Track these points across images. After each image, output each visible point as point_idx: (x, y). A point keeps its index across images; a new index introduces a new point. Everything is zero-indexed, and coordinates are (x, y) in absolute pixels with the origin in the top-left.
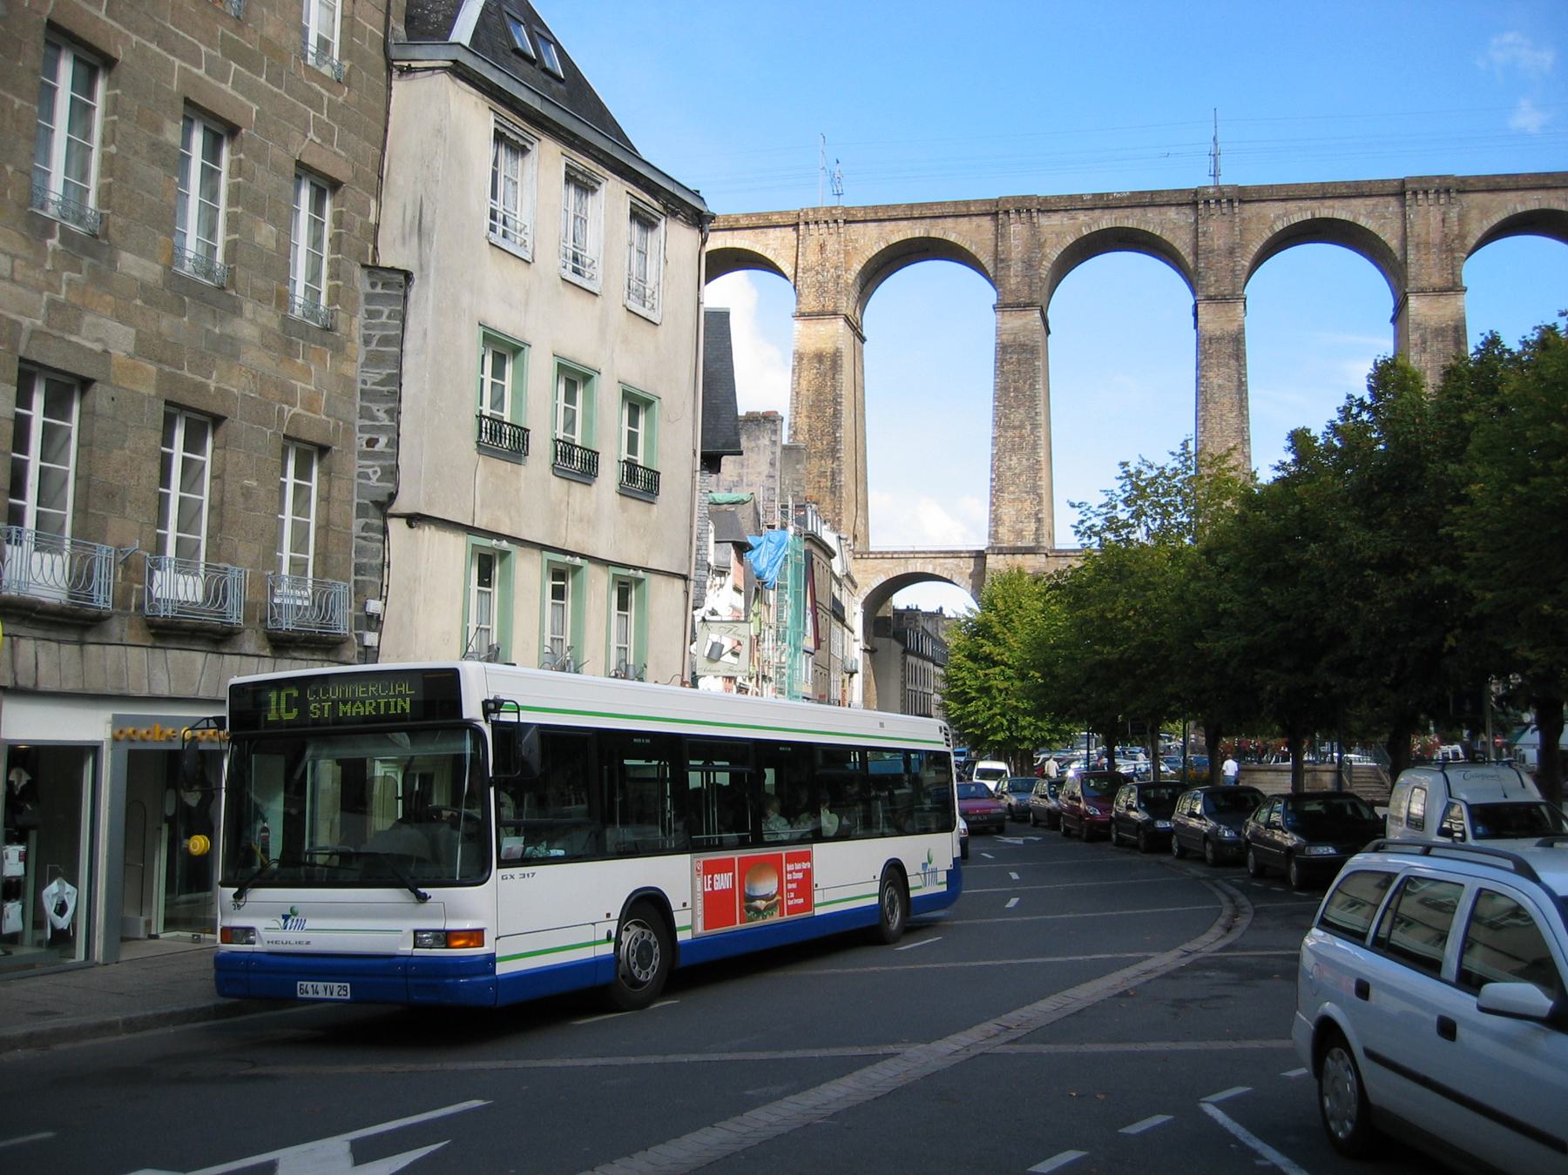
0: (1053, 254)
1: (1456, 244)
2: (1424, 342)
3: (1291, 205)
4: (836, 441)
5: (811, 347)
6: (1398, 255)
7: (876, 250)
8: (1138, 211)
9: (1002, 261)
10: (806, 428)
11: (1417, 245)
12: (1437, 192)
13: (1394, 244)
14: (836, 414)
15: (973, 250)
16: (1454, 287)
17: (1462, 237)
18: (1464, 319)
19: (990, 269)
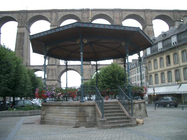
0: (60, 18)
1: (121, 18)
3: (97, 12)
4: (23, 47)
5: (20, 32)
6: (113, 19)
7: (31, 17)
8: (73, 12)
9: (51, 19)
10: (18, 45)
11: (116, 18)
12: (118, 11)
13: (112, 18)
14: (23, 43)
15: (47, 17)
17: (122, 17)
19: (50, 21)
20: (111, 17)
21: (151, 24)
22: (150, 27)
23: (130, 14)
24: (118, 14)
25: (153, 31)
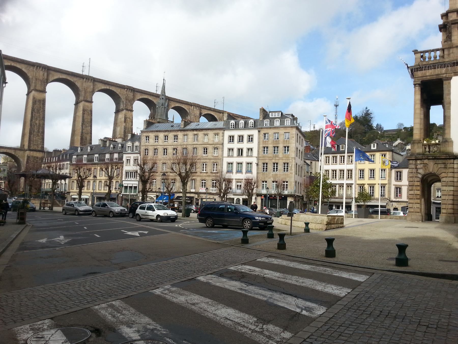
2: (35, 102)
12: (42, 68)
13: (30, 77)
16: (44, 91)
18: (45, 99)
20: (30, 75)
21: (89, 99)
22: (87, 104)
23: (61, 77)
24: (41, 73)
25: (91, 111)
